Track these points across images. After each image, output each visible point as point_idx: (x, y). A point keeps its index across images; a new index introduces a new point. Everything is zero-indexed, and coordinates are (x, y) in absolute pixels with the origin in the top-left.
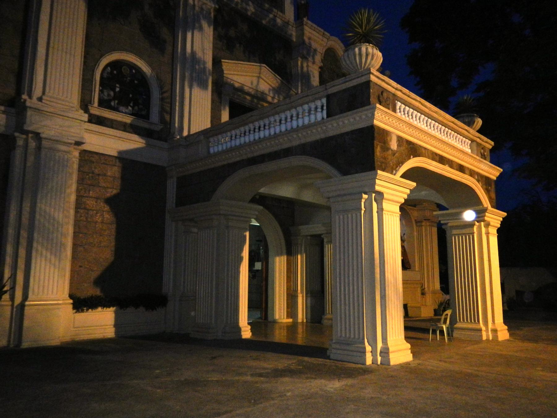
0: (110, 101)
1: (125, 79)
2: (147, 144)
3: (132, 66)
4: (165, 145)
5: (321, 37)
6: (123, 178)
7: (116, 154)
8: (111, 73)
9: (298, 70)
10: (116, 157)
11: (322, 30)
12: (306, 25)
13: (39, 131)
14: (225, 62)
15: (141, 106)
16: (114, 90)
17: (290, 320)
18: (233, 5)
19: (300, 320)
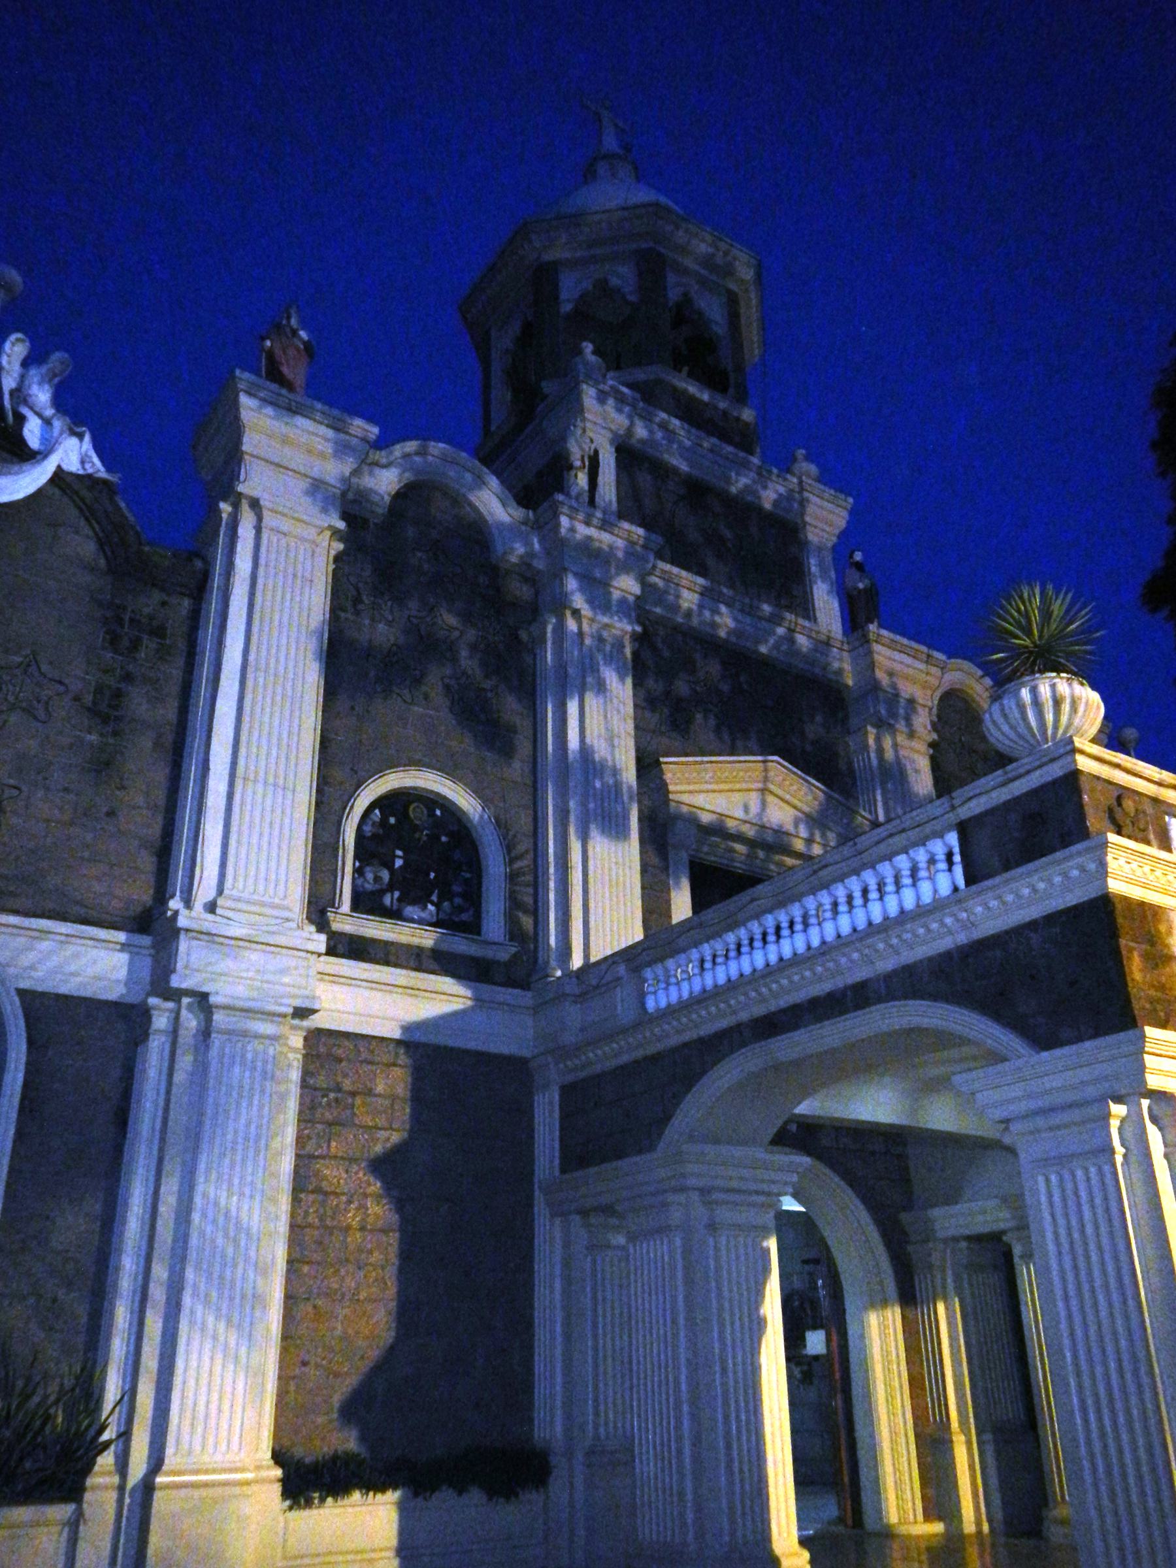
0: (382, 892)
1: (417, 835)
2: (477, 999)
3: (431, 801)
4: (525, 998)
5: (922, 666)
6: (418, 1097)
7: (396, 1034)
8: (384, 822)
9: (869, 758)
10: (398, 1042)
11: (924, 649)
12: (876, 642)
13: (205, 989)
14: (671, 763)
15: (458, 901)
16: (389, 865)
17: (938, 1528)
18: (680, 620)
19: (969, 1527)
